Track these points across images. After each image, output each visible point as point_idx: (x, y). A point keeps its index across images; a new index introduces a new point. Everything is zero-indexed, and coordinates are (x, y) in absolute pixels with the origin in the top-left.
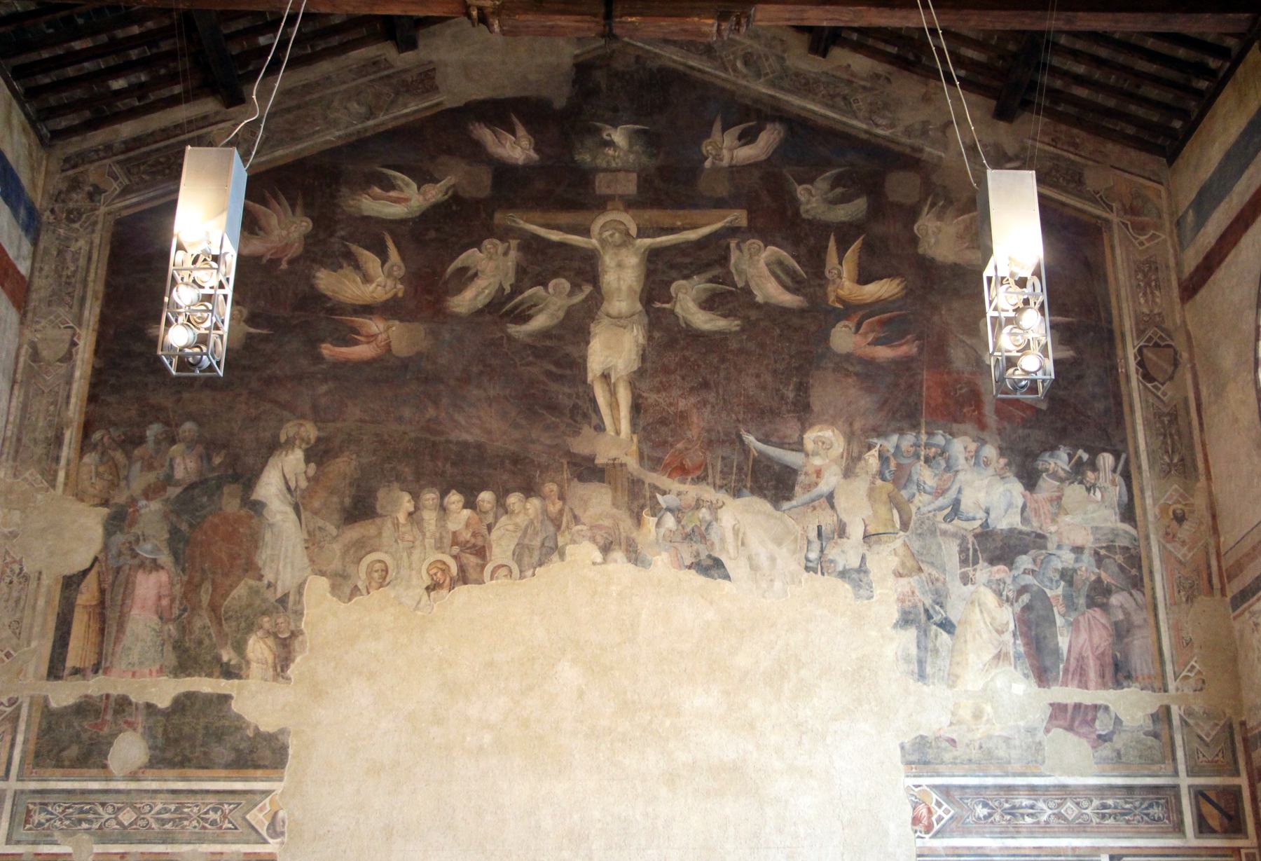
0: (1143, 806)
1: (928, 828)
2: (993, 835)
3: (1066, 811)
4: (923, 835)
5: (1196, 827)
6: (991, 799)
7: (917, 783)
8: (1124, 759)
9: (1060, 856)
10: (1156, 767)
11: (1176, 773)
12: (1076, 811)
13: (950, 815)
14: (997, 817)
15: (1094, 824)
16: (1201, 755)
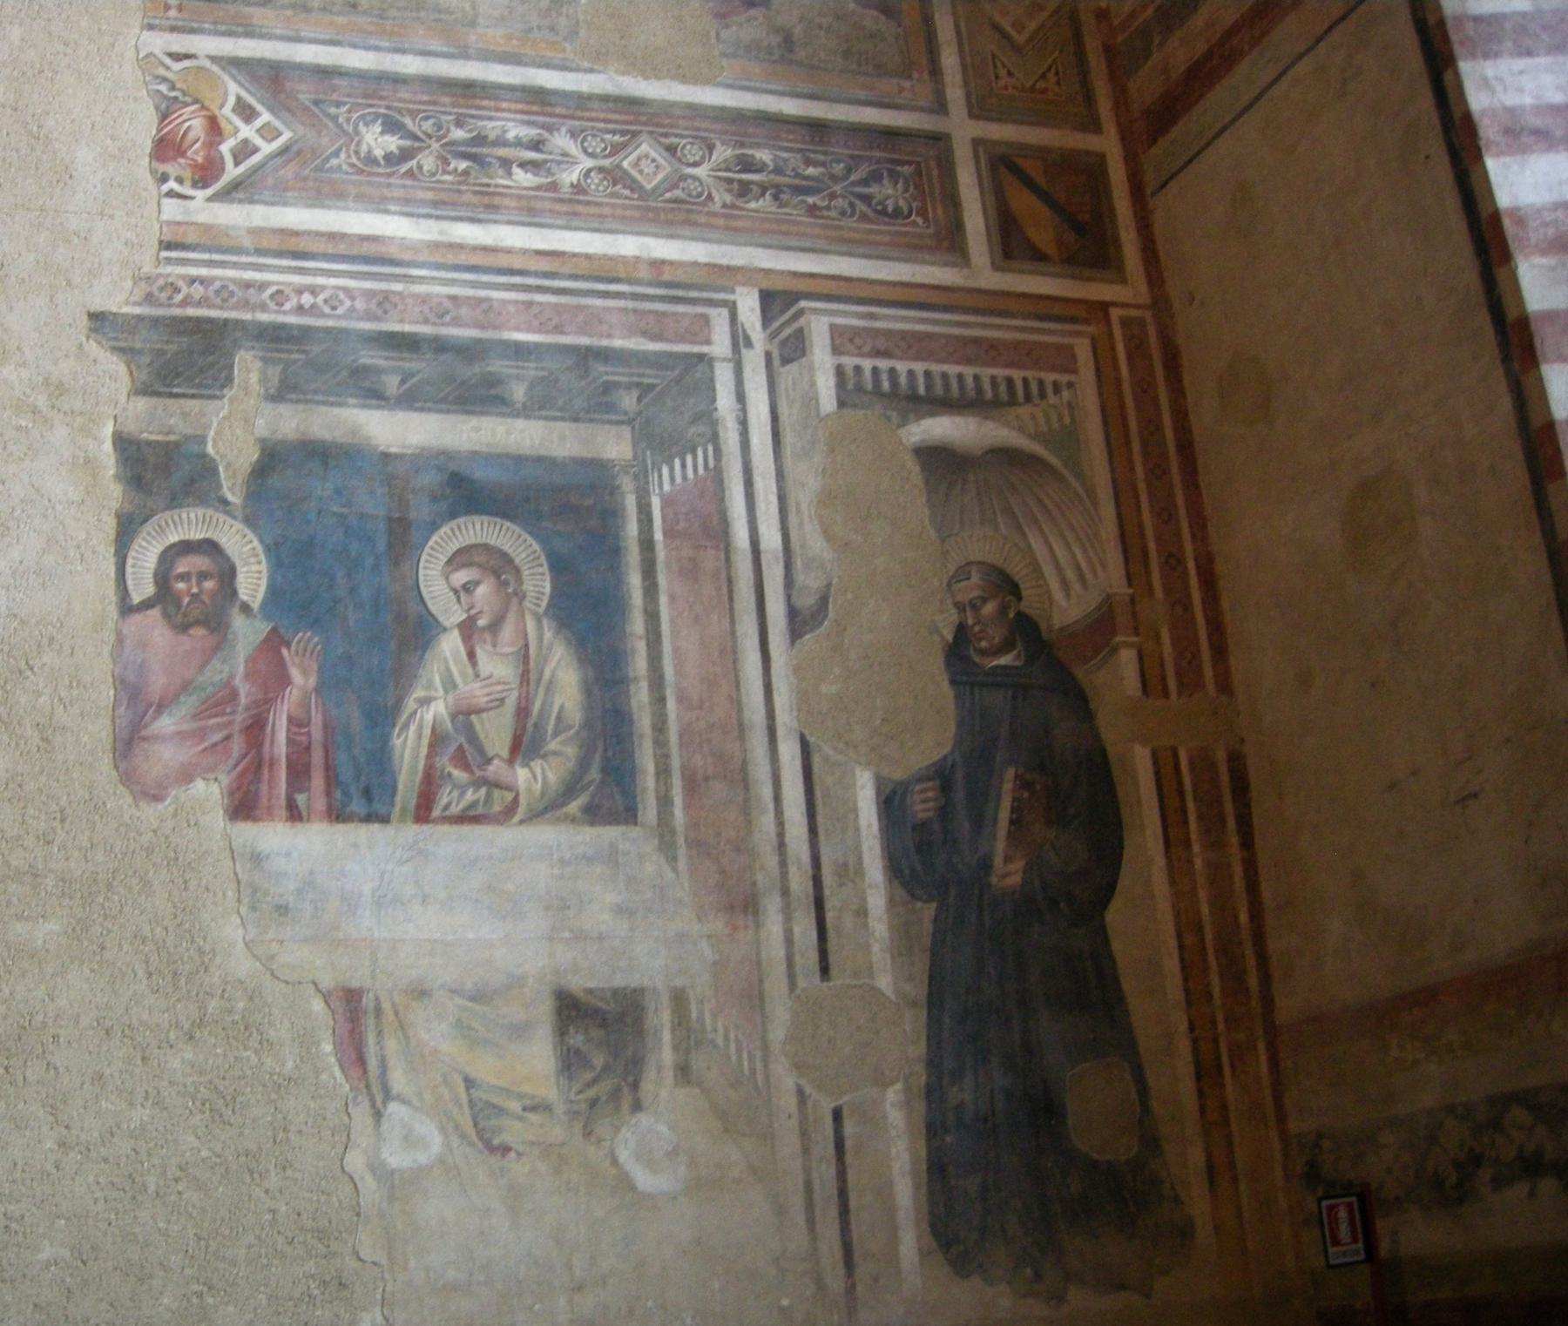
0: (853, 178)
1: (206, 173)
3: (636, 164)
4: (186, 190)
5: (996, 238)
6: (413, 114)
7: (176, 48)
8: (801, 54)
10: (889, 85)
11: (941, 107)
12: (667, 168)
14: (428, 162)
15: (717, 206)
16: (1002, 72)
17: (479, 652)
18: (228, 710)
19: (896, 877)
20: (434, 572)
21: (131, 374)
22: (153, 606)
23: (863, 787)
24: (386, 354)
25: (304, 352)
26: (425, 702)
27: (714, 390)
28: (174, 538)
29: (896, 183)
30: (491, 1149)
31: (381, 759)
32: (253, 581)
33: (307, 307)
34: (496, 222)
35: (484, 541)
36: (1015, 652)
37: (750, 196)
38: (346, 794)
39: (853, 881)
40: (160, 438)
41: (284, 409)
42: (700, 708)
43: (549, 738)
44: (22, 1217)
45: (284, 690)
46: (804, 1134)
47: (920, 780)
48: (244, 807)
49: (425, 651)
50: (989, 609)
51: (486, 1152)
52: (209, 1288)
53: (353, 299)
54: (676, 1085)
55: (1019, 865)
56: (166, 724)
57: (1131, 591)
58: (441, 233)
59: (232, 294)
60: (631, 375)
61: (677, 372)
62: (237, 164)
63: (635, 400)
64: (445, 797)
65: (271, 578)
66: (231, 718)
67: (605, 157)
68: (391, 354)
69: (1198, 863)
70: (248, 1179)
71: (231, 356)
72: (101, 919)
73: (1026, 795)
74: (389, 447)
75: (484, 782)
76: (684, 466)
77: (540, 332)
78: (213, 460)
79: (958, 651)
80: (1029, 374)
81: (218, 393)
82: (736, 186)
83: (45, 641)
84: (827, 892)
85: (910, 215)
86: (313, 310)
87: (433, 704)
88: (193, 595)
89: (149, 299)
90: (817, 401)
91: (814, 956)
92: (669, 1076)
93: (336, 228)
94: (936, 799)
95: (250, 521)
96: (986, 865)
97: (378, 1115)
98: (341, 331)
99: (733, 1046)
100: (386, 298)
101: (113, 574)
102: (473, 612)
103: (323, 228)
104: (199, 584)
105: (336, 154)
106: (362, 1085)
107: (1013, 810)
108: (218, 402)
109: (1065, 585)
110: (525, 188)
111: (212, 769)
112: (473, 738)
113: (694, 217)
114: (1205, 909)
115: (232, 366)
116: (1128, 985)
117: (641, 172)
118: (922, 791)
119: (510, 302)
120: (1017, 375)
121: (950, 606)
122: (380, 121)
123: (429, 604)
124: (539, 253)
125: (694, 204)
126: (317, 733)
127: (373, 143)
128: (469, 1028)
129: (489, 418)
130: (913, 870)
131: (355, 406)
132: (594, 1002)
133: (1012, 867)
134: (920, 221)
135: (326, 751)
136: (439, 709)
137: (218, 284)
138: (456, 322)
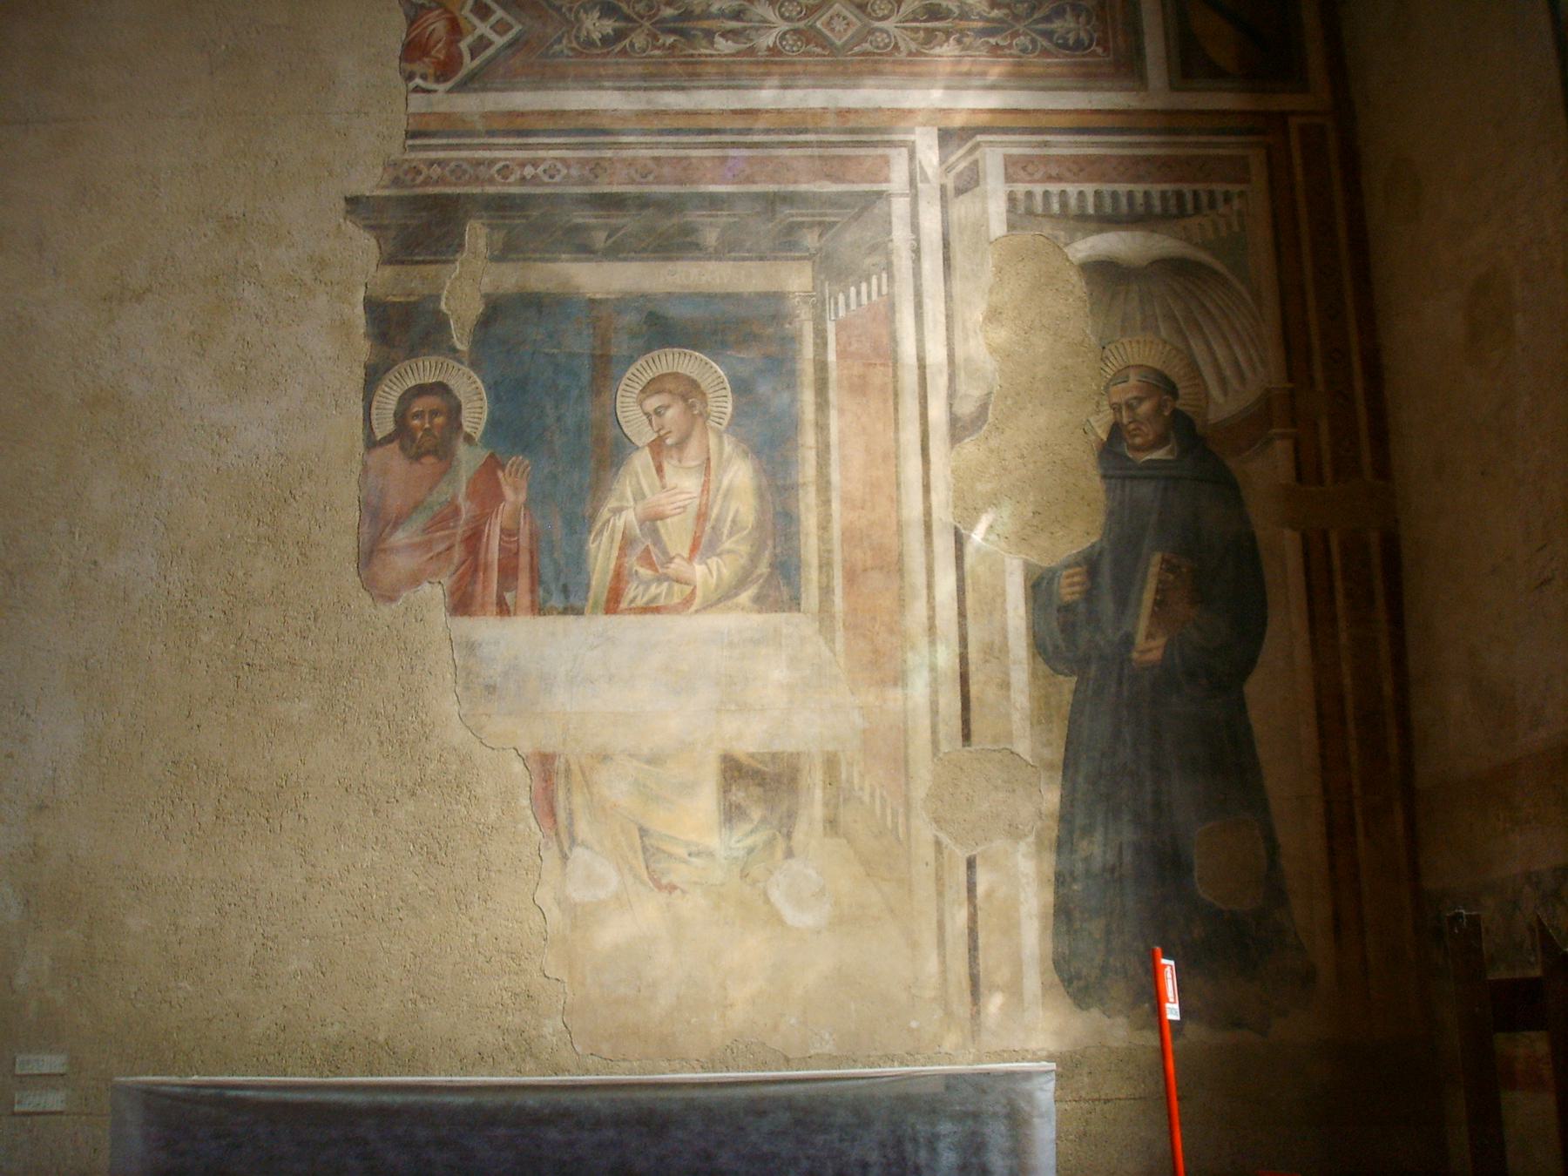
1: (446, 70)
2: (622, 83)
3: (829, 23)
4: (431, 85)
9: (806, 131)
13: (510, 35)
14: (639, 40)
17: (668, 468)
18: (452, 524)
19: (1040, 654)
20: (631, 400)
21: (380, 248)
22: (391, 441)
23: (1011, 573)
24: (596, 213)
25: (527, 217)
26: (618, 511)
27: (890, 223)
28: (411, 383)
29: (1078, 16)
30: (660, 887)
31: (578, 560)
32: (475, 414)
33: (529, 177)
34: (699, 88)
35: (675, 370)
36: (1167, 448)
37: (934, 42)
38: (548, 592)
39: (998, 658)
40: (402, 299)
41: (506, 268)
42: (863, 508)
43: (724, 537)
44: (276, 937)
45: (499, 506)
46: (939, 879)
47: (1067, 567)
48: (462, 604)
49: (619, 469)
50: (1145, 408)
51: (656, 890)
52: (422, 996)
53: (568, 167)
54: (825, 835)
55: (1160, 641)
56: (400, 537)
57: (1290, 385)
58: (649, 102)
59: (465, 172)
60: (813, 216)
61: (857, 210)
62: (473, 58)
63: (816, 237)
64: (632, 591)
65: (491, 413)
66: (454, 531)
67: (799, 20)
68: (601, 213)
69: (1343, 638)
70: (457, 910)
71: (464, 225)
72: (344, 700)
73: (1171, 577)
74: (595, 293)
75: (667, 578)
76: (858, 293)
77: (733, 183)
78: (444, 314)
79: (1112, 451)
80: (1199, 186)
81: (452, 258)
82: (922, 34)
83: (306, 473)
84: (972, 668)
85: (1090, 45)
86: (535, 180)
87: (624, 513)
88: (426, 429)
89: (396, 182)
90: (988, 227)
91: (957, 724)
92: (819, 827)
93: (556, 107)
94: (1083, 584)
95: (473, 365)
96: (1128, 641)
97: (565, 858)
98: (556, 195)
99: (878, 802)
100: (597, 164)
101: (361, 416)
102: (662, 433)
103: (545, 108)
104: (431, 422)
105: (559, 41)
106: (553, 834)
107: (1157, 591)
108: (453, 266)
109: (1223, 381)
110: (726, 55)
111: (435, 574)
112: (657, 540)
113: (880, 67)
114: (1347, 681)
115: (463, 235)
116: (1263, 752)
117: (833, 30)
118: (1068, 577)
119: (706, 158)
120: (1187, 188)
121: (1107, 407)
122: (598, 8)
123: (625, 430)
124: (735, 112)
125: (881, 54)
126: (524, 541)
127: (592, 27)
128: (644, 786)
129: (686, 263)
130: (1056, 647)
131: (567, 261)
132: (754, 764)
133: (1153, 644)
134: (1099, 50)
135: (532, 557)
136: (629, 517)
137: (453, 164)
138: (659, 180)
